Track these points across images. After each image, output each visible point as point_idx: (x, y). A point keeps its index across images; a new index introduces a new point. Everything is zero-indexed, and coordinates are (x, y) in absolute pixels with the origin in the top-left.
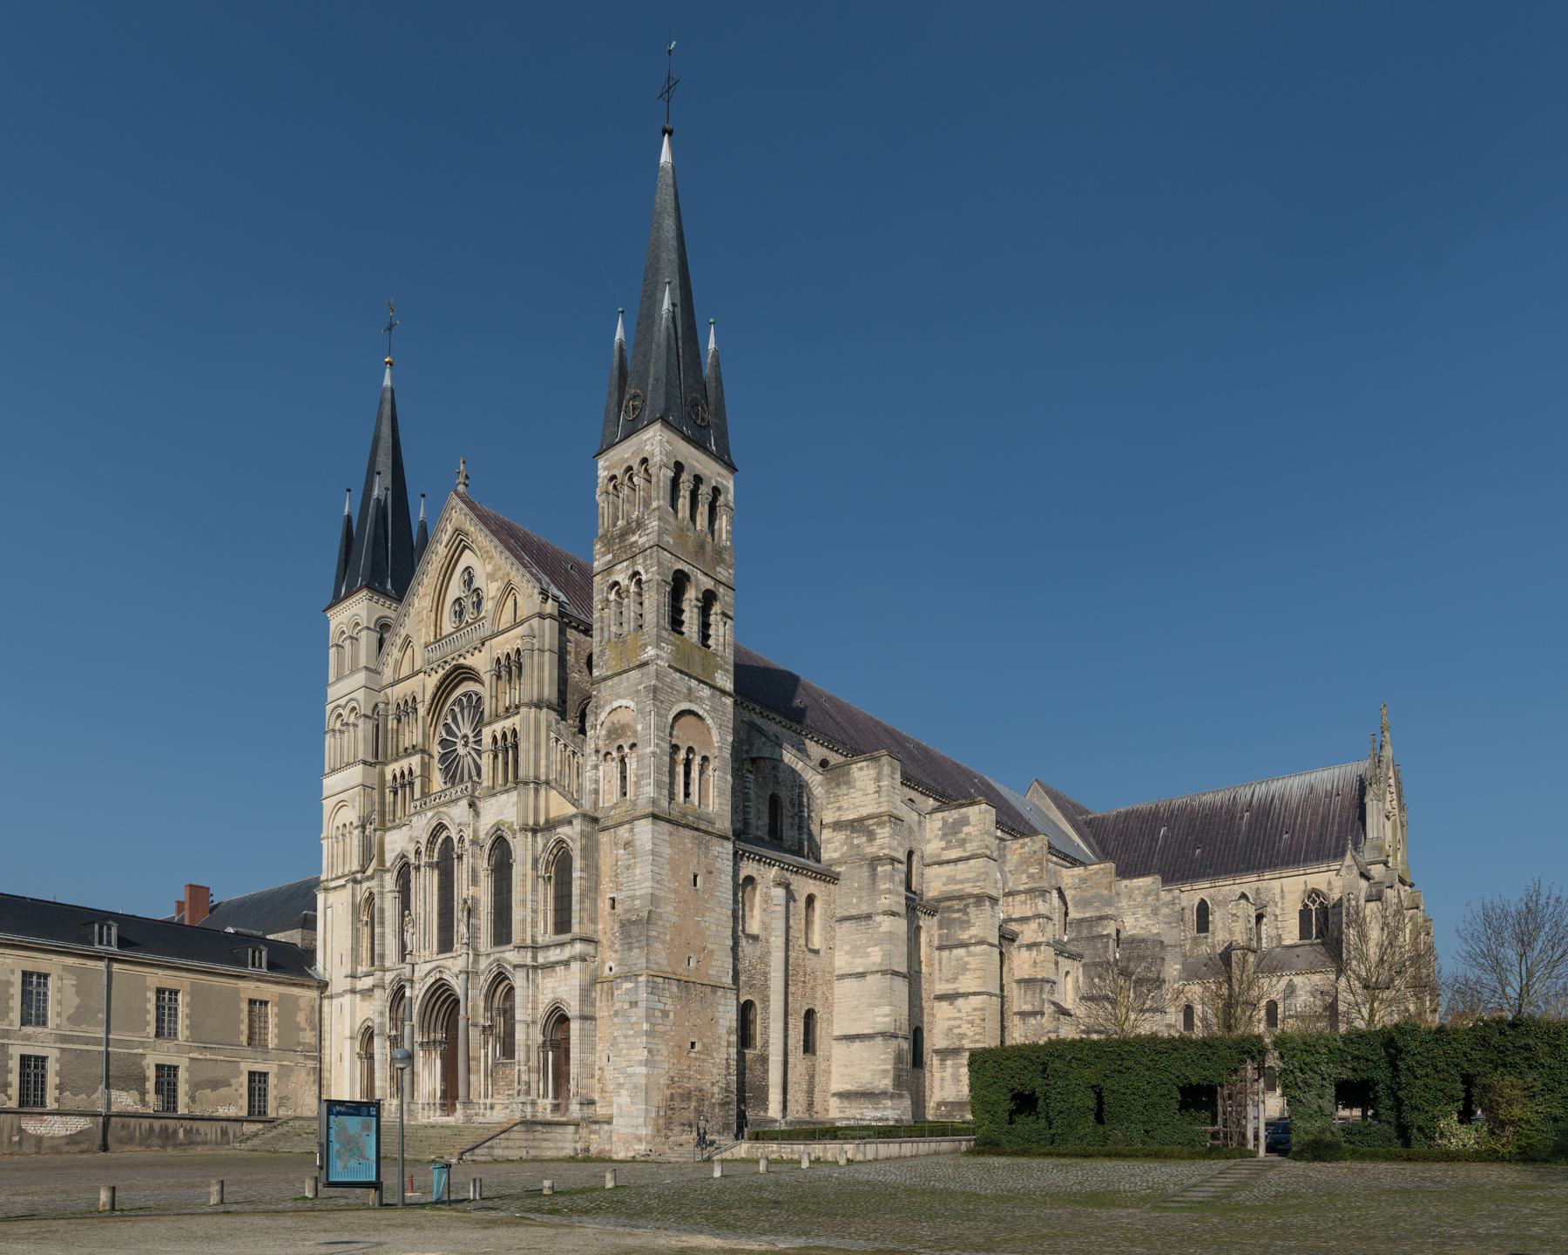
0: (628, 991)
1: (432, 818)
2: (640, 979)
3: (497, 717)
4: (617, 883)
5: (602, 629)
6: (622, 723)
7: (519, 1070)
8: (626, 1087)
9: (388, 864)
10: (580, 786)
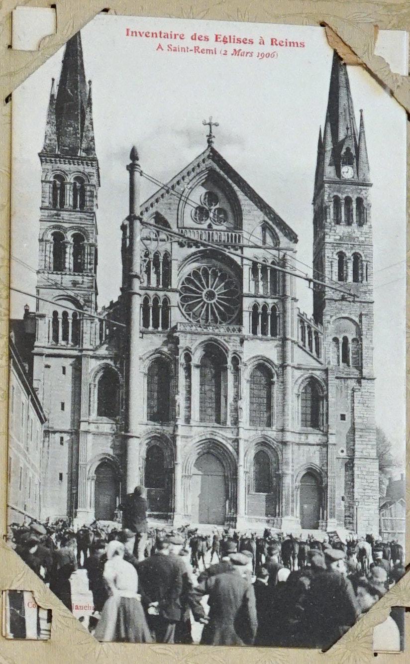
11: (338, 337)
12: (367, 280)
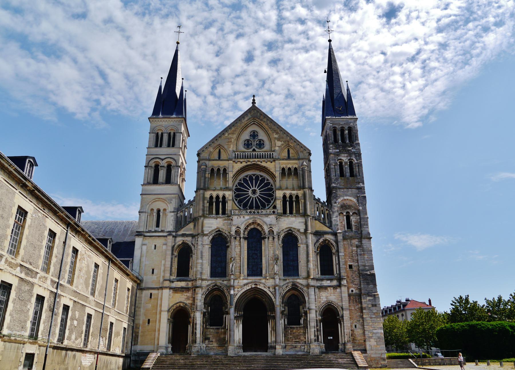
0: (369, 300)
1: (248, 219)
2: (376, 296)
3: (280, 188)
4: (353, 260)
5: (335, 171)
6: (348, 204)
7: (315, 331)
8: (373, 338)
9: (205, 233)
10: (331, 222)
11: (343, 212)
12: (359, 175)
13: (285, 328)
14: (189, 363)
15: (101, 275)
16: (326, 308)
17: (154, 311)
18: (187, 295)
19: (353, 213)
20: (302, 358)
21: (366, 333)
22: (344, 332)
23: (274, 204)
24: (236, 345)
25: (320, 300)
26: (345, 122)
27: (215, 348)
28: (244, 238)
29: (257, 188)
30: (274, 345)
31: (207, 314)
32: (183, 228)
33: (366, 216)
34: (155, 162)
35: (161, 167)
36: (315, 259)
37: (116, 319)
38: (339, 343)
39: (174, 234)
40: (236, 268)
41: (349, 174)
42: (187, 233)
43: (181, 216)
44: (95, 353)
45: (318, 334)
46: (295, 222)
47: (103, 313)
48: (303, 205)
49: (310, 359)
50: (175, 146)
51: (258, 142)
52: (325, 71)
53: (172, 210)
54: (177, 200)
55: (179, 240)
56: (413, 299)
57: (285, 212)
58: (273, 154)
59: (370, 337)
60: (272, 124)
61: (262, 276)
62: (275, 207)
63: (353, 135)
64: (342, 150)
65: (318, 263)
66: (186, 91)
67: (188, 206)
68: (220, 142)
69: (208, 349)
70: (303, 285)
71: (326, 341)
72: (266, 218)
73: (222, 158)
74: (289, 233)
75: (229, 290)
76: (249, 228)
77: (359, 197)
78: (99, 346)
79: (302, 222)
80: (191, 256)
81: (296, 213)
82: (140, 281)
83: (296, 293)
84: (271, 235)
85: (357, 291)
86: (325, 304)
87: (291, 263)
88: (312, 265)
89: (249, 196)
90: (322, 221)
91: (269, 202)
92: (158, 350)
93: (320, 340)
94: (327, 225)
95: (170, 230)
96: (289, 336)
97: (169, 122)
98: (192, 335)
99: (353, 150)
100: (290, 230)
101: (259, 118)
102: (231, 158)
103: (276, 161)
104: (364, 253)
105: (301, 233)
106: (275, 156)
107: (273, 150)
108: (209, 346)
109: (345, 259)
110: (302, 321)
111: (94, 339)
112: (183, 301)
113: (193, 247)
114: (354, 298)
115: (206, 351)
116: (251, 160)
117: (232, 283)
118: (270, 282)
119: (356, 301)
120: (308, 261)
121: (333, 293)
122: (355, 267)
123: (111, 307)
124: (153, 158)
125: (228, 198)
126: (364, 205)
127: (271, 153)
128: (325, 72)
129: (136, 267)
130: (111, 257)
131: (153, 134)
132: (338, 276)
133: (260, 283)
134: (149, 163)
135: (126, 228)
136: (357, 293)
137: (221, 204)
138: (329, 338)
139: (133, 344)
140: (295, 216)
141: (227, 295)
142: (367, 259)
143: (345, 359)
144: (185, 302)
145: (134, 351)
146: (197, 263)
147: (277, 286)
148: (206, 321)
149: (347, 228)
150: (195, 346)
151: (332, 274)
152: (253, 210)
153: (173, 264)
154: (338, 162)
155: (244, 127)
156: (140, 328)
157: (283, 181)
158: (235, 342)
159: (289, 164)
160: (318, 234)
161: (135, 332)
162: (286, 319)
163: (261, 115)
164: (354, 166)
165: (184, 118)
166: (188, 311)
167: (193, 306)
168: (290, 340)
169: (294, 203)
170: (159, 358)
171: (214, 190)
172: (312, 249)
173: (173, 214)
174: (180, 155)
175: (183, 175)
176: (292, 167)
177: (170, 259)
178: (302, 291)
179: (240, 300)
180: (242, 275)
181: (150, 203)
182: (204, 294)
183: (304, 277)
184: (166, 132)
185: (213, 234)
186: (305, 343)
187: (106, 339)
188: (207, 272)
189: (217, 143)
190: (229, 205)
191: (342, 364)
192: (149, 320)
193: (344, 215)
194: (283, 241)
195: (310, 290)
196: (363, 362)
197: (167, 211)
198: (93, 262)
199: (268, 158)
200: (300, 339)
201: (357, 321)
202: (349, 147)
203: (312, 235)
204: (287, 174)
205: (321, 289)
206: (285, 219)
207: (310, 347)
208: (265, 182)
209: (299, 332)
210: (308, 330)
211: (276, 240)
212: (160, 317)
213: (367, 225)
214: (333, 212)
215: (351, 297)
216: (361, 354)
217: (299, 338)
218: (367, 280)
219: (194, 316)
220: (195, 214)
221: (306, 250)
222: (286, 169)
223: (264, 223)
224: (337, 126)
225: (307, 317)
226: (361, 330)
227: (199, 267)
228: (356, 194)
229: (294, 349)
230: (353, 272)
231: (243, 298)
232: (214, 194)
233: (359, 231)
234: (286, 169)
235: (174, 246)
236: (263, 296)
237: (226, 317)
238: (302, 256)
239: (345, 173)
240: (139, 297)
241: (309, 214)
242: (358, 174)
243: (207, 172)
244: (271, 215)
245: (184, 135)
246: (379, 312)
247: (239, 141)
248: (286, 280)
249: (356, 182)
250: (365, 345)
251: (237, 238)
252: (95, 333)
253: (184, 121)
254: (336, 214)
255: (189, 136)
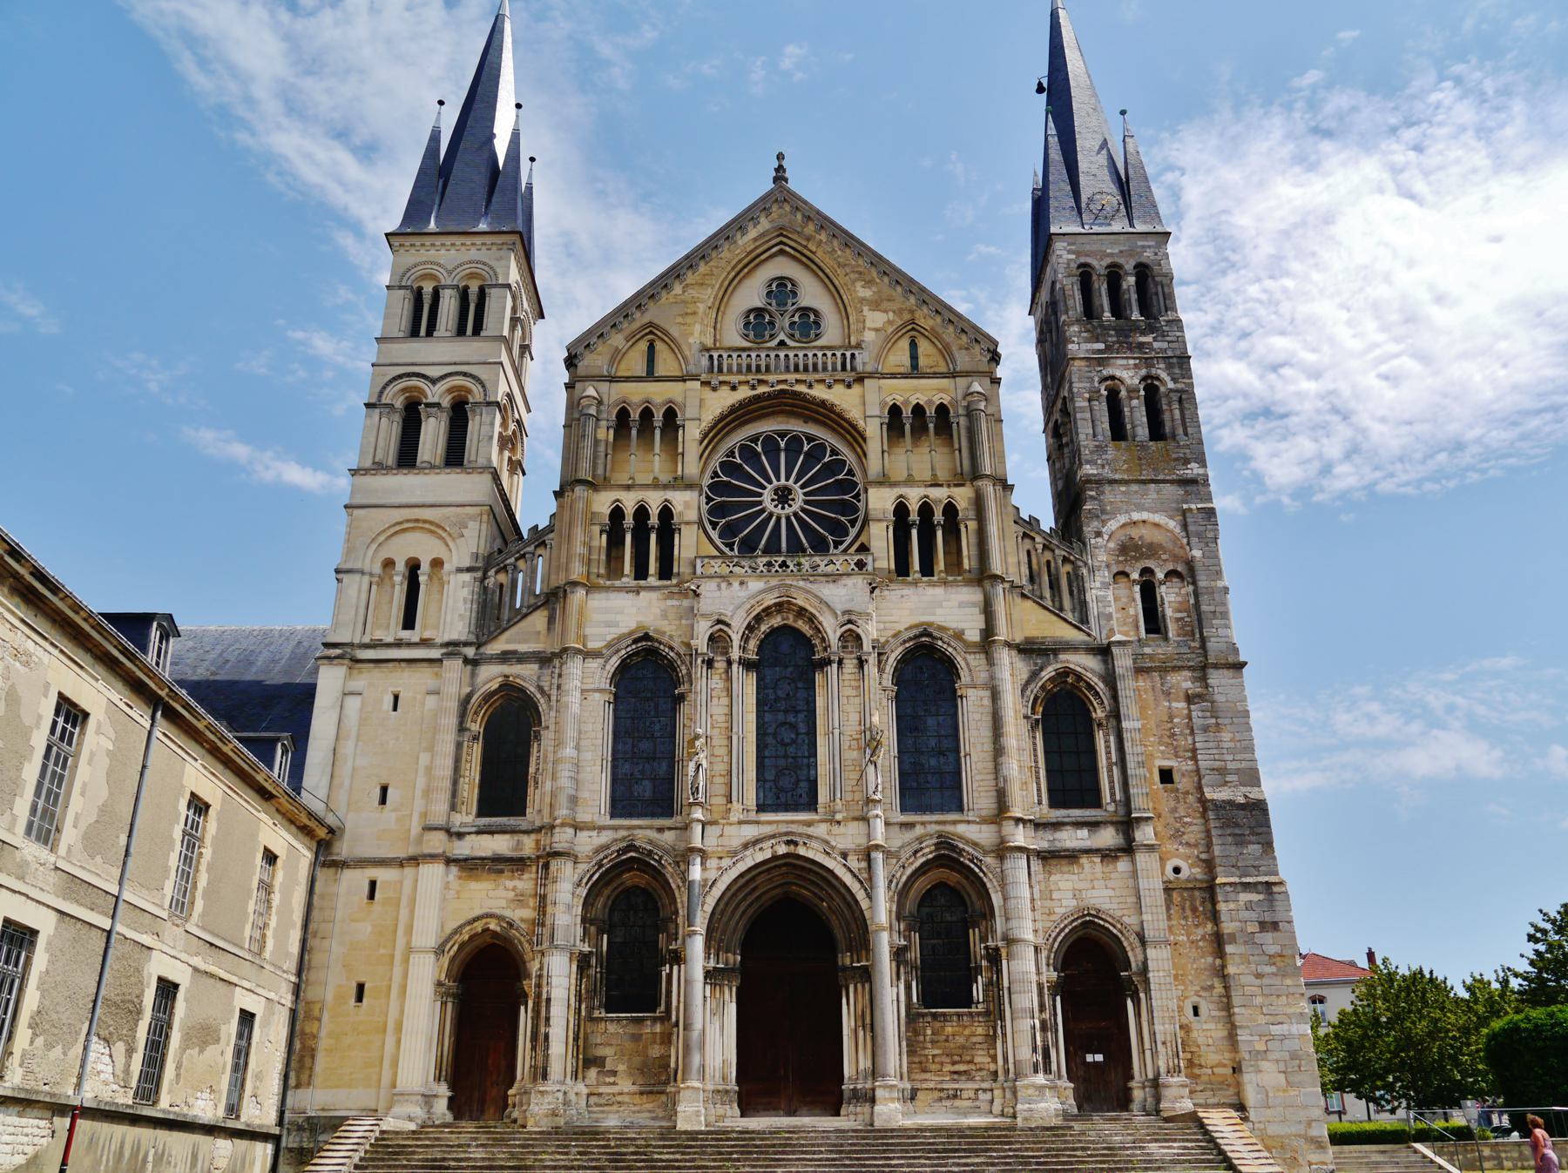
0: (1249, 906)
2: (1275, 889)
3: (884, 481)
6: (1148, 539)
7: (1034, 1027)
8: (1270, 1056)
10: (1082, 607)
11: (1127, 569)
12: (1186, 434)
13: (912, 1018)
14: (508, 1159)
15: (103, 763)
16: (1075, 937)
17: (382, 951)
18: (513, 890)
19: (1171, 574)
20: (989, 1137)
21: (1243, 1036)
22: (1153, 1034)
23: (863, 539)
24: (710, 1087)
25: (1048, 903)
26: (1122, 248)
27: (626, 1099)
28: (742, 662)
29: (795, 483)
30: (869, 1085)
31: (593, 961)
32: (506, 629)
33: (1220, 584)
34: (404, 390)
35: (428, 405)
36: (1027, 745)
37: (196, 970)
38: (1132, 1078)
39: (470, 652)
40: (710, 780)
41: (1147, 430)
42: (523, 648)
43: (501, 585)
44: (58, 1109)
45: (1044, 1040)
46: (944, 604)
47: (109, 933)
48: (973, 540)
49: (1022, 1143)
50: (482, 334)
51: (796, 319)
52: (1040, 84)
53: (467, 563)
54: (484, 526)
55: (490, 676)
56: (1313, 951)
57: (902, 568)
58: (853, 355)
59: (1258, 1052)
60: (848, 251)
61: (816, 810)
62: (864, 548)
63: (1157, 294)
64: (1114, 343)
65: (1036, 762)
66: (532, 159)
67: (528, 549)
68: (652, 314)
69: (597, 1105)
70: (982, 847)
71: (1077, 1070)
72: (831, 585)
73: (660, 371)
74: (922, 646)
75: (683, 867)
76: (764, 628)
77: (1188, 515)
78: (80, 1077)
79: (974, 605)
80: (536, 737)
81: (947, 570)
82: (331, 831)
83: (953, 878)
84: (851, 652)
85: (1198, 870)
86: (1073, 921)
87: (933, 762)
88: (1015, 766)
89: (763, 511)
90: (1048, 603)
91: (839, 531)
92: (389, 1108)
93: (1054, 1067)
94: (1070, 617)
95: (454, 636)
96: (927, 1052)
97: (463, 248)
98: (534, 1048)
99: (1156, 345)
100: (926, 633)
101: (799, 229)
102: (694, 372)
103: (866, 381)
104: (1220, 721)
105: (967, 644)
106: (864, 364)
107: (853, 342)
108: (602, 1090)
109: (1145, 746)
110: (978, 991)
111: (49, 1046)
112: (498, 912)
113: (542, 701)
114: (1184, 899)
115: (589, 1112)
116: (771, 378)
117: (697, 843)
118: (849, 836)
119: (1194, 910)
120: (998, 751)
121: (1100, 875)
122: (1183, 775)
123: (164, 915)
124: (400, 377)
125: (681, 514)
126: (1211, 542)
127: (848, 354)
128: (1040, 89)
129: (314, 776)
130: (163, 693)
131: (402, 292)
132: (1121, 811)
133: (809, 837)
134: (381, 393)
135: (302, 650)
136: (1196, 880)
137: (653, 537)
138: (1089, 1058)
139: (292, 1082)
140: (945, 583)
141: (674, 886)
142: (1231, 745)
143: (1175, 1141)
144: (508, 913)
145: (293, 1111)
146: (555, 762)
147: (877, 847)
148: (592, 993)
149: (1148, 631)
150: (542, 1093)
151: (1097, 803)
152: (780, 559)
153: (464, 766)
154: (1103, 388)
155: (745, 261)
156: (325, 1018)
157: (893, 457)
158: (707, 1076)
159: (916, 390)
160: (1030, 649)
161: (303, 1033)
162: (914, 984)
163: (809, 218)
164: (1164, 401)
165: (520, 233)
166: (518, 951)
167: (538, 930)
168: (933, 1067)
169: (939, 534)
170: (384, 1139)
171: (628, 488)
172: (1014, 704)
173: (467, 577)
174: (501, 363)
175: (513, 444)
176: (930, 402)
177: (450, 748)
178: (977, 870)
179: (727, 904)
180: (736, 806)
181: (382, 538)
182: (585, 881)
183: (984, 813)
184: (449, 283)
185: (623, 652)
186: (995, 1080)
187: (130, 1052)
188: (596, 797)
189: (640, 319)
190: (688, 543)
191: (1163, 1161)
192: (361, 988)
193: (1134, 581)
194: (898, 677)
195: (1008, 864)
196: (1257, 1155)
197: (447, 566)
198: (47, 686)
199: (834, 369)
200: (971, 1062)
201: (1203, 988)
202: (1143, 333)
203: (1014, 653)
204: (908, 427)
205: (1054, 862)
206: (905, 592)
207: (1015, 1092)
208: (826, 460)
209: (967, 1032)
210: (1003, 1027)
211: (871, 668)
212: (405, 976)
213: (1225, 615)
214: (1092, 571)
215: (1175, 894)
216: (1239, 1121)
217: (968, 1058)
218: (1237, 825)
219: (541, 969)
220: (553, 577)
221: (989, 709)
222: (907, 412)
223: (825, 609)
224: (1094, 262)
225: (999, 972)
226: (1220, 1026)
227: (567, 774)
228: (1177, 502)
229: (948, 1103)
230: (1179, 796)
231: (741, 896)
232: (629, 502)
233: (1193, 640)
234: (907, 412)
235: (469, 696)
236: (822, 889)
237: (670, 976)
238: (974, 733)
239: (1129, 426)
240: (322, 897)
241: (999, 573)
242: (1180, 431)
243: (603, 423)
244: (849, 575)
245: (518, 301)
246: (1290, 952)
247: (724, 313)
248: (911, 825)
249: (1176, 460)
250: (1238, 1085)
251: (716, 665)
252: (54, 1016)
253: (519, 247)
254: (1104, 575)
255: (543, 317)
